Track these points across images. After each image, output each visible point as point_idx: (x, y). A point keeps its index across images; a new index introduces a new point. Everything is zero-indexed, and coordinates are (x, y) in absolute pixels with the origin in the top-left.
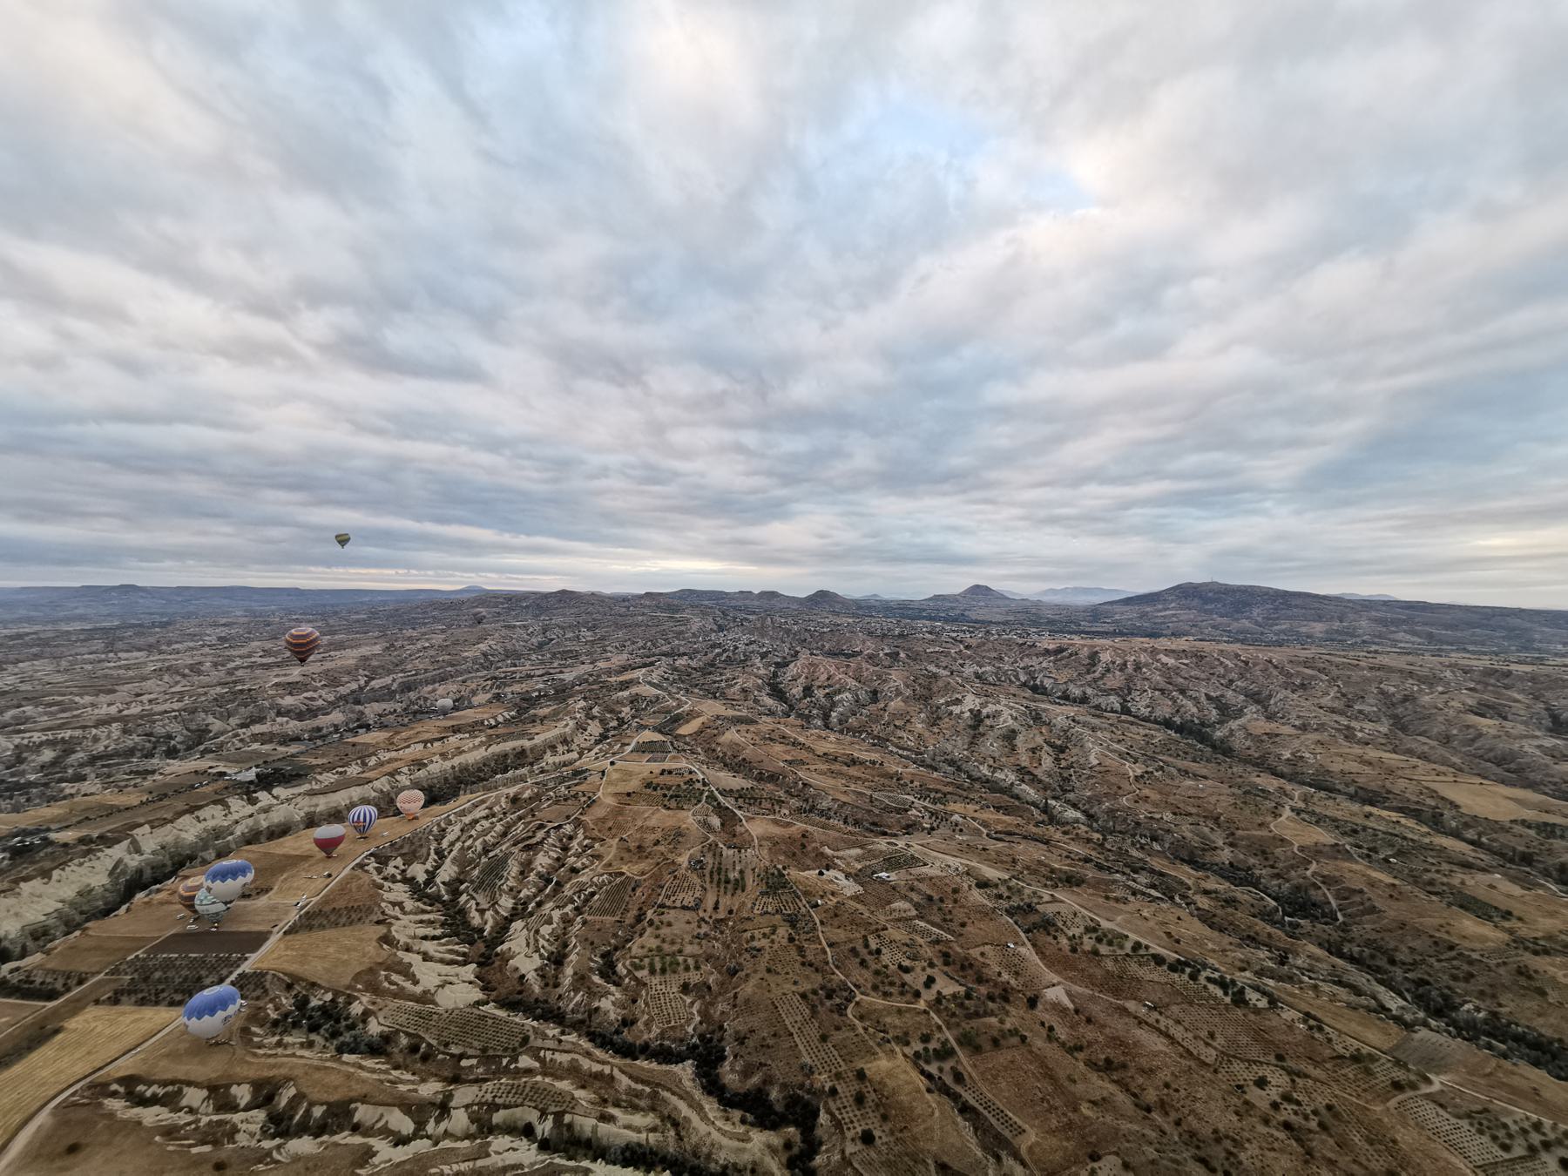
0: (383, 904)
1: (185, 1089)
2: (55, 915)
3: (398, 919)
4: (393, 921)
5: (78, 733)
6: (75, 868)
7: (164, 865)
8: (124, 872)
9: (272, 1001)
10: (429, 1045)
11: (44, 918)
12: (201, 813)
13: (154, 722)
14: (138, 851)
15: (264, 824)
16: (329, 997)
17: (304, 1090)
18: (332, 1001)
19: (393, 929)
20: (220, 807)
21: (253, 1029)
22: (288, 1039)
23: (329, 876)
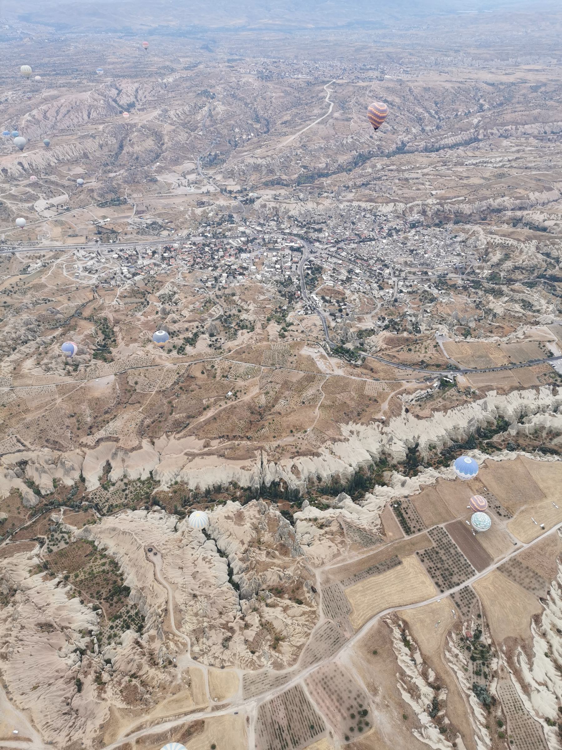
0: (554, 583)
1: (418, 651)
2: (441, 438)
3: (554, 602)
4: (550, 603)
5: (515, 243)
6: (456, 411)
7: (493, 423)
8: (473, 425)
9: (468, 621)
10: (506, 730)
11: (436, 439)
12: (524, 393)
13: (554, 244)
14: (485, 408)
15: (548, 425)
16: (489, 641)
17: (448, 702)
18: (490, 645)
19: (544, 612)
20: (534, 391)
21: (454, 635)
22: (461, 656)
23: (543, 528)
